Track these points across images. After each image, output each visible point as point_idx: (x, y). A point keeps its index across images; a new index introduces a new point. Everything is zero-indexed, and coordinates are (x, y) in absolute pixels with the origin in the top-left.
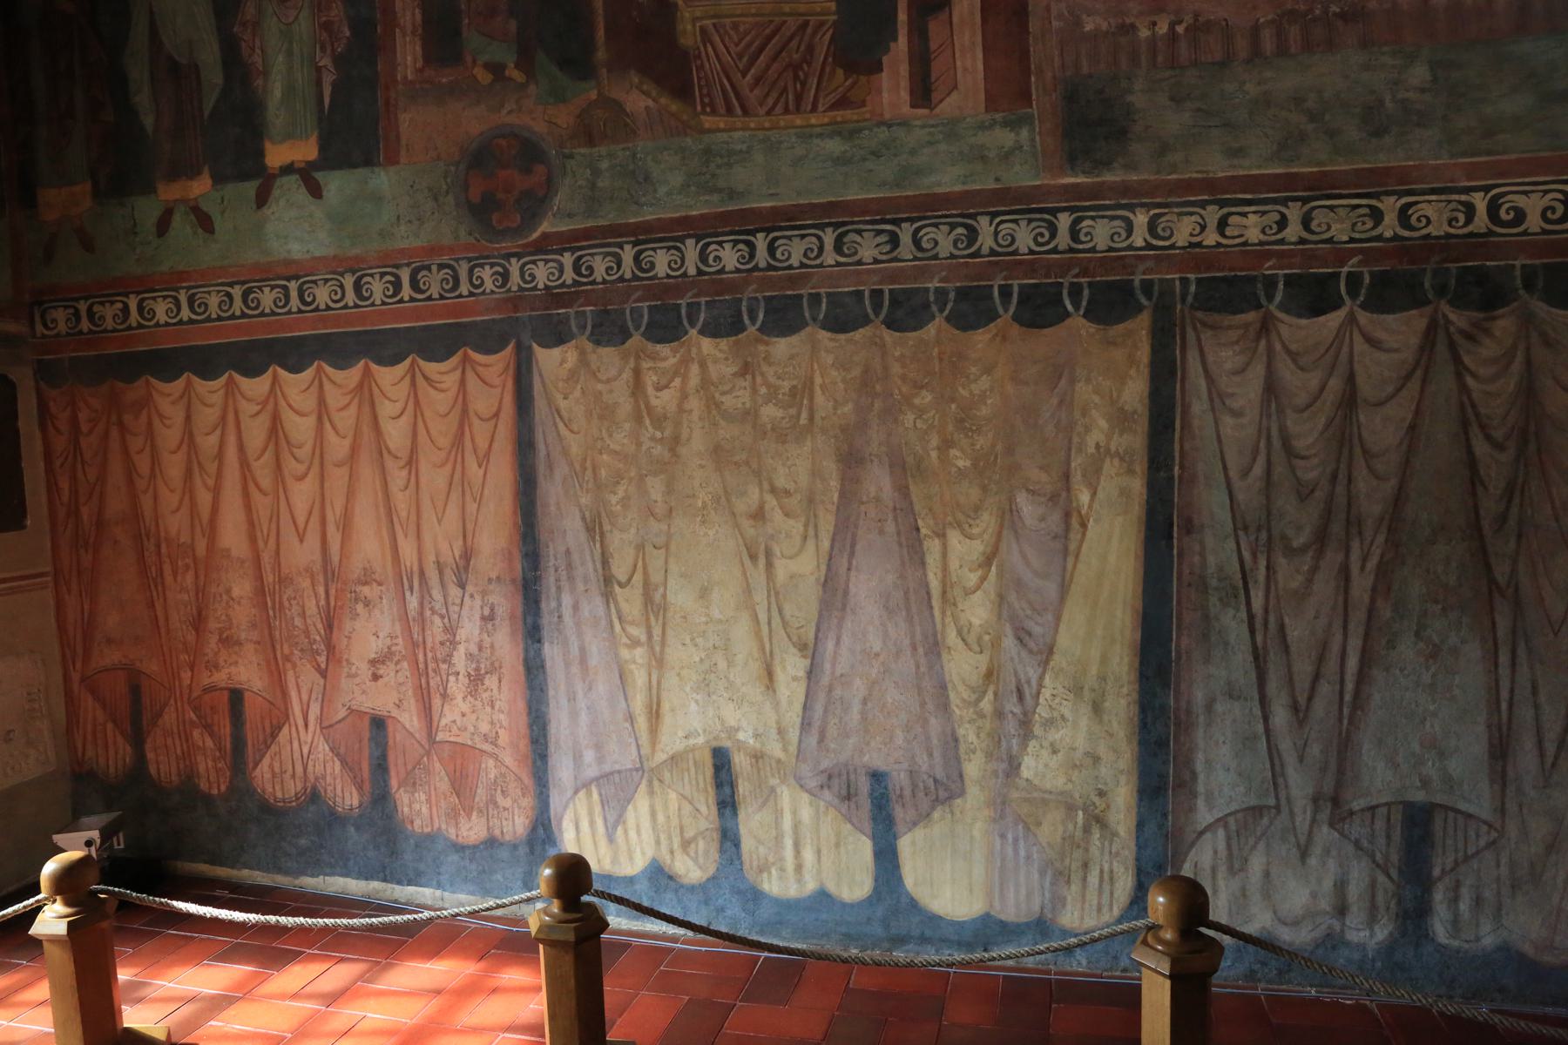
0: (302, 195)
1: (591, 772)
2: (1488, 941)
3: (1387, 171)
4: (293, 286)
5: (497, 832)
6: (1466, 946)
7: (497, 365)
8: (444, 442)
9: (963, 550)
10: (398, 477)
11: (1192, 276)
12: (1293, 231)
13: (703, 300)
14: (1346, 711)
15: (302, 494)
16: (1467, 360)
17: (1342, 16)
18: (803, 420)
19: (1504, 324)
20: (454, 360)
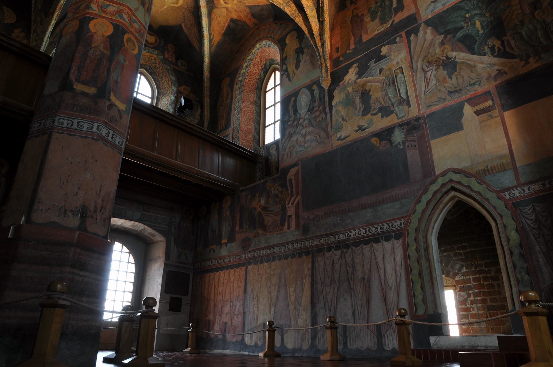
0: (225, 247)
1: (249, 328)
2: (355, 347)
3: (336, 232)
4: (223, 259)
5: (238, 340)
6: (352, 348)
7: (243, 268)
8: (237, 280)
9: (292, 289)
10: (232, 285)
11: (316, 249)
12: (327, 241)
13: (266, 258)
14: (335, 310)
15: (221, 289)
16: (346, 256)
17: (331, 213)
18: (275, 273)
19: (350, 251)
20: (239, 268)
